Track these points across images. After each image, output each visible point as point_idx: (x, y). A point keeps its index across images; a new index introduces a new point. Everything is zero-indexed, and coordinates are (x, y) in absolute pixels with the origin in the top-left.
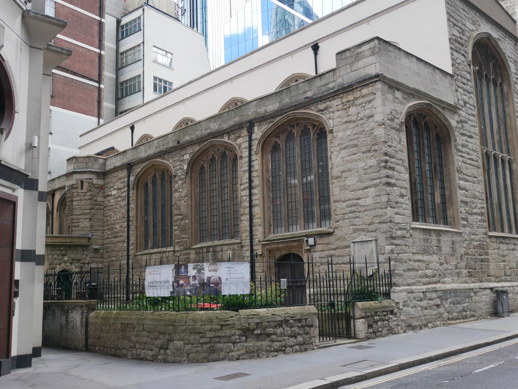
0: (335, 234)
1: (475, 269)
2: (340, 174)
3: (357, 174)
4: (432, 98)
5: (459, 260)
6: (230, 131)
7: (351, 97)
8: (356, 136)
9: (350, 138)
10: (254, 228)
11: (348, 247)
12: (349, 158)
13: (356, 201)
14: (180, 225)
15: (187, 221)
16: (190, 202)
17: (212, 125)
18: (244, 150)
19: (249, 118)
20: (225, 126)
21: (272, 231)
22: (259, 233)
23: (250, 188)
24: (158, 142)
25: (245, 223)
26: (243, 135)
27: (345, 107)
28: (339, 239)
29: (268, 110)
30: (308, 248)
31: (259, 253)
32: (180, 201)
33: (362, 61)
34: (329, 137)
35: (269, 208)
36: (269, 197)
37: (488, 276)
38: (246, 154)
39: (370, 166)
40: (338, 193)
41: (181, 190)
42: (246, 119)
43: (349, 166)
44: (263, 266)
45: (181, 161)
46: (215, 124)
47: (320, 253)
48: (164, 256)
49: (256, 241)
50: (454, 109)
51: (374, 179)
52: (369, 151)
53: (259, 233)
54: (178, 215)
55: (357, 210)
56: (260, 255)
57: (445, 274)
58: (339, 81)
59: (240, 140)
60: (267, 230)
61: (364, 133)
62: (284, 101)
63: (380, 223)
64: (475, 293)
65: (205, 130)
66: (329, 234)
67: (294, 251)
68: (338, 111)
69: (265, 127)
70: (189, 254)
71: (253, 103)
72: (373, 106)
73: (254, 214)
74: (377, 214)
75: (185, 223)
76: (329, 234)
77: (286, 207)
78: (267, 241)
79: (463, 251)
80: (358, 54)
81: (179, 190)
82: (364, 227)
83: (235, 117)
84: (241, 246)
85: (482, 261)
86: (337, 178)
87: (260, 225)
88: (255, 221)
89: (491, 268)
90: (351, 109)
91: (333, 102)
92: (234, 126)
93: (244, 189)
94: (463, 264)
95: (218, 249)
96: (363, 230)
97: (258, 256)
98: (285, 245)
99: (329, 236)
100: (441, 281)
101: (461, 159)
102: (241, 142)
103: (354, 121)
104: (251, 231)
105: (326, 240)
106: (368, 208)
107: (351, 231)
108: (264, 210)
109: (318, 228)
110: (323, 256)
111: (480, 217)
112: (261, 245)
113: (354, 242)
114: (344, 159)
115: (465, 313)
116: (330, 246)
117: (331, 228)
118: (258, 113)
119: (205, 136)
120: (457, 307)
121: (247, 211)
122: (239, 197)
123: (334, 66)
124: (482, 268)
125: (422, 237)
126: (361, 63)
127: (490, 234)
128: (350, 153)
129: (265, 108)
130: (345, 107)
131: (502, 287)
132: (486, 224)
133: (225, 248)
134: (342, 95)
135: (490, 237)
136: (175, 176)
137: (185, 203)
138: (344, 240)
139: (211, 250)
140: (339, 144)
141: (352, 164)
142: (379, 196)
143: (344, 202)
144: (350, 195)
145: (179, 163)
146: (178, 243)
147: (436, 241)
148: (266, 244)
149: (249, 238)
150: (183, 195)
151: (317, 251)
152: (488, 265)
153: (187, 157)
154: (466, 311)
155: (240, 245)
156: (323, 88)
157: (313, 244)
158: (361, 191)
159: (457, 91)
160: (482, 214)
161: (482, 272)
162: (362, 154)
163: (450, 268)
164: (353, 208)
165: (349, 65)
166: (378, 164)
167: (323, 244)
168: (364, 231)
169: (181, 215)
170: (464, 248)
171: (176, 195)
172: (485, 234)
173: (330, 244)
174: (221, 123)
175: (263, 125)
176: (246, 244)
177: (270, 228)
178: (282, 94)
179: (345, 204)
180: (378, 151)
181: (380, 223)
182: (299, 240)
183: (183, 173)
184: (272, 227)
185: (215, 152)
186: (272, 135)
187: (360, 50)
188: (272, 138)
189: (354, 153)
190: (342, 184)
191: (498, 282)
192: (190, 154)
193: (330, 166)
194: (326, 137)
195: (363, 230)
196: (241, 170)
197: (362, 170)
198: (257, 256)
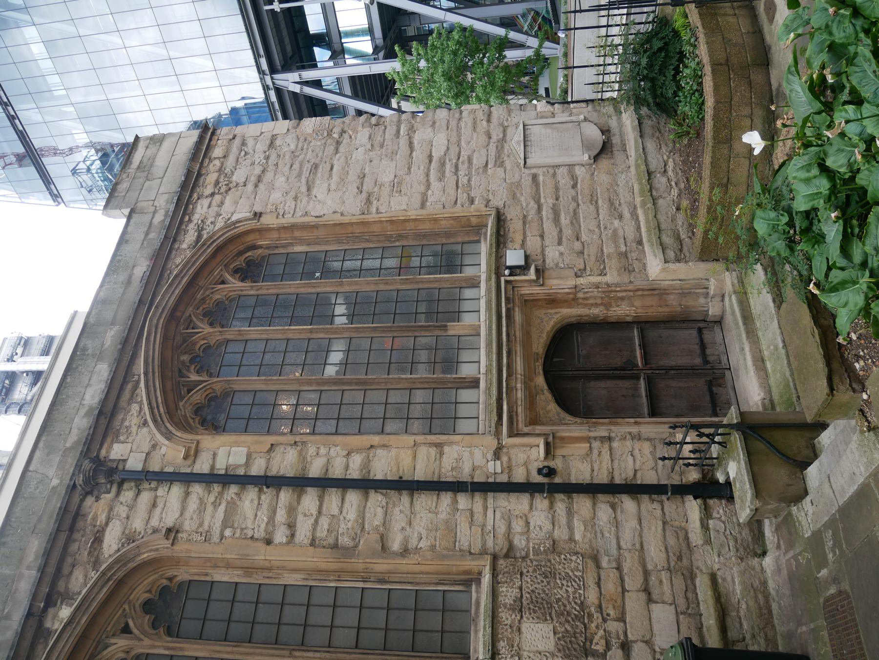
2: (364, 195)
3: (375, 162)
6: (53, 584)
8: (296, 166)
9: (295, 173)
10: (449, 476)
12: (335, 178)
13: (433, 164)
18: (154, 522)
22: (468, 453)
23: (300, 483)
25: (417, 524)
28: (514, 196)
39: (370, 138)
40: (405, 199)
43: (352, 177)
44: (588, 439)
47: (547, 242)
49: (493, 469)
51: (398, 131)
52: (338, 143)
53: (466, 455)
55: (454, 161)
61: (297, 154)
63: (489, 121)
66: (500, 219)
67: (539, 345)
74: (470, 124)
76: (500, 219)
80: (139, 167)
82: (492, 148)
84: (506, 556)
86: (369, 201)
96: (500, 149)
97: (552, 464)
98: (518, 348)
99: (504, 221)
102: (123, 522)
103: (263, 171)
106: (454, 139)
107: (500, 171)
110: (555, 233)
114: (333, 187)
116: (530, 218)
128: (327, 175)
129: (83, 411)
130: (223, 190)
138: (518, 185)
140: (296, 199)
141: (350, 172)
142: (434, 123)
143: (428, 186)
144: (418, 173)
155: (501, 562)
156: (152, 236)
158: (414, 154)
162: (338, 155)
164: (449, 167)
166: (371, 126)
168: (503, 147)
173: (525, 217)
175: (123, 420)
178: (85, 349)
179: (435, 185)
180: (346, 129)
181: (489, 121)
186: (172, 406)
188: (177, 407)
189: (329, 169)
190: (386, 190)
193: (338, 218)
195: (500, 149)
196: (216, 538)
197: (371, 153)
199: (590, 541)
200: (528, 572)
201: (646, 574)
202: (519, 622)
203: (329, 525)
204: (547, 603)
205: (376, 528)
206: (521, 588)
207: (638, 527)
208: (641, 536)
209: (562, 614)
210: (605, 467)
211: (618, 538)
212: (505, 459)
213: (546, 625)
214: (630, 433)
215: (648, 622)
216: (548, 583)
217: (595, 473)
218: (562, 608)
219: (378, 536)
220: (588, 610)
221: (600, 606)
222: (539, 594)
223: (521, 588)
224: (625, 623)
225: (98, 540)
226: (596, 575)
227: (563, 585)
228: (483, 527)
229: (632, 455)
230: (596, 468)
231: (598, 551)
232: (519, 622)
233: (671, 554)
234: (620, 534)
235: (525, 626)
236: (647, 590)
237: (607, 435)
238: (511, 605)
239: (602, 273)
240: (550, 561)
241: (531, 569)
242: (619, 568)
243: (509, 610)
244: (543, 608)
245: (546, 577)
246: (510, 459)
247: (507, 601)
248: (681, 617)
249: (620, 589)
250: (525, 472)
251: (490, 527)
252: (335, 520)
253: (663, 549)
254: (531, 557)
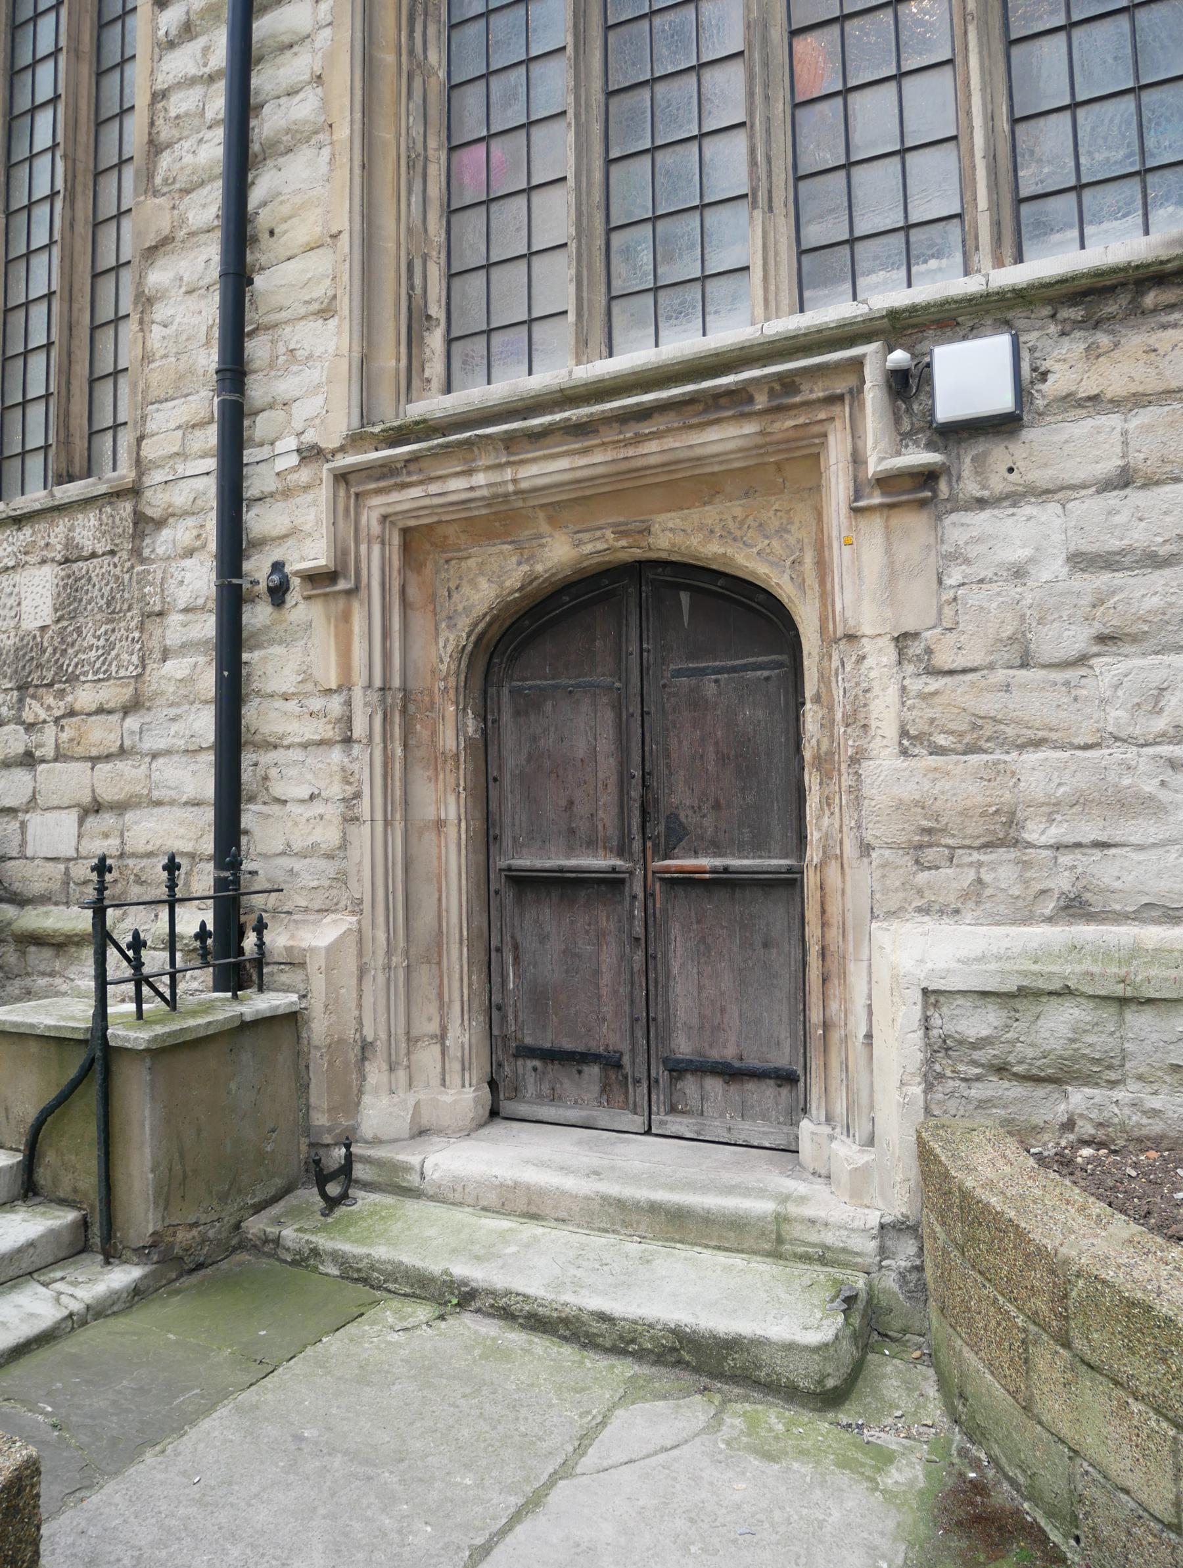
21: (435, 369)
30: (919, 457)
31: (313, 553)
35: (416, 163)
36: (416, 68)
44: (345, 686)
47: (1089, 507)
53: (315, 375)
56: (318, 579)
60: (389, 360)
67: (678, 534)
73: (263, 219)
77: (597, 129)
78: (398, 436)
84: (140, 519)
87: (326, 312)
88: (279, 282)
93: (188, 30)
98: (597, 459)
104: (234, 372)
108: (367, 167)
109: (999, 263)
112: (324, 493)
121: (207, 208)
122: (140, 98)
148: (385, 471)
149: (210, 437)
155: (126, 508)
176: (180, 497)
177: (413, 339)
182: (788, 384)
184: (435, 340)
198: (278, 594)
199: (162, 693)
200: (115, 566)
201: (120, 807)
202: (53, 560)
203: (187, 114)
204: (75, 610)
205: (183, 221)
206: (94, 555)
207: (184, 799)
208: (172, 803)
209: (63, 641)
210: (289, 729)
211: (168, 752)
212: (304, 476)
213: (50, 610)
214: (357, 795)
215: (56, 803)
216: (100, 608)
217: (279, 703)
218: (69, 640)
219: (166, 232)
220: (69, 689)
221: (72, 713)
222: (87, 592)
223: (94, 555)
224: (56, 760)
226: (111, 705)
227: (99, 638)
228: (182, 455)
229: (312, 797)
230: (292, 706)
231: (149, 709)
232: (53, 560)
233: (144, 862)
234: (175, 758)
236: (95, 807)
237: (355, 737)
238: (73, 538)
239: (910, 740)
240: (129, 609)
241: (118, 571)
242: (122, 752)
243: (67, 537)
244: (69, 603)
245: (109, 604)
246: (306, 488)
247: (78, 530)
248: (62, 867)
249: (94, 753)
250: (275, 533)
251: (181, 470)
252: (197, 121)
253: (150, 848)
254: (139, 568)
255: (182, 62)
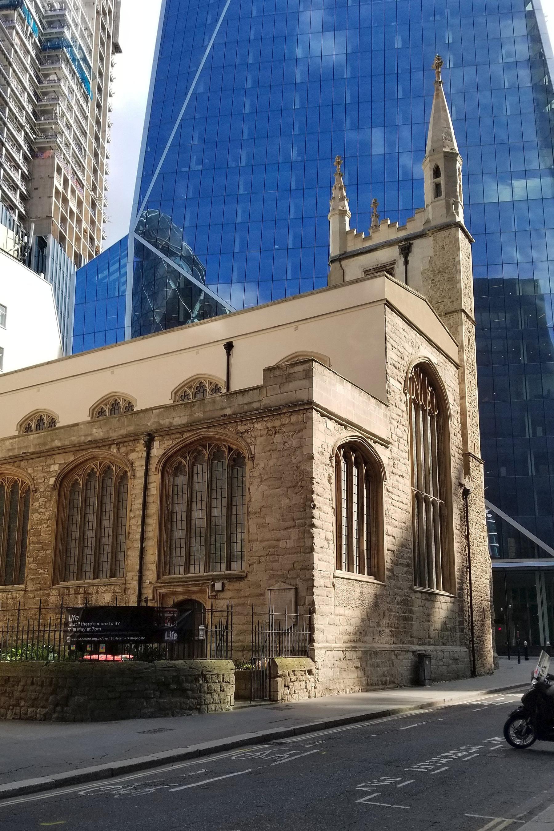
0: (249, 578)
1: (398, 628)
4: (365, 431)
5: (382, 616)
6: (121, 443)
7: (277, 423)
11: (263, 595)
14: (37, 557)
15: (48, 552)
16: (54, 527)
17: (95, 431)
19: (147, 430)
20: (114, 435)
21: (168, 571)
23: (144, 516)
24: (11, 444)
26: (138, 449)
27: (270, 432)
29: (175, 424)
32: (41, 524)
33: (294, 382)
34: (249, 465)
37: (411, 637)
38: (140, 473)
41: (43, 510)
42: (143, 429)
45: (47, 472)
46: (100, 430)
48: (10, 596)
50: (386, 444)
53: (152, 572)
54: (35, 543)
57: (366, 632)
58: (266, 401)
59: (132, 456)
62: (196, 416)
64: (396, 656)
65: (85, 436)
67: (194, 597)
68: (261, 436)
69: (168, 443)
70: (49, 594)
71: (154, 411)
72: (302, 437)
75: (46, 554)
78: (162, 583)
79: (386, 606)
80: (289, 374)
81: (39, 511)
83: (128, 426)
84: (125, 588)
85: (406, 619)
89: (414, 628)
90: (276, 436)
91: (256, 425)
92: (126, 436)
94: (385, 622)
95: (92, 590)
100: (362, 640)
101: (390, 501)
105: (236, 585)
111: (405, 569)
112: (152, 588)
113: (270, 590)
115: (385, 678)
117: (243, 572)
118: (160, 425)
119: (85, 444)
120: (377, 671)
121: (137, 545)
122: (127, 525)
123: (260, 382)
124: (405, 628)
125: (344, 587)
126: (292, 386)
127: (416, 588)
129: (171, 420)
130: (270, 432)
131: (425, 651)
132: (411, 577)
133: (101, 589)
134: (268, 418)
135: (416, 592)
136: (36, 491)
137: (48, 529)
139: (82, 591)
143: (261, 542)
145: (42, 475)
146: (33, 580)
147: (359, 594)
149: (137, 578)
150: (45, 517)
151: (224, 599)
152: (412, 625)
153: (55, 468)
154: (386, 676)
155: (123, 586)
156: (246, 407)
157: (220, 589)
159: (390, 423)
160: (408, 565)
161: (405, 631)
163: (371, 625)
165: (278, 385)
167: (231, 590)
169: (40, 543)
170: (387, 603)
171: (34, 517)
172: (411, 588)
174: (108, 431)
175: (166, 440)
176: (132, 586)
177: (165, 567)
179: (263, 544)
182: (203, 584)
183: (48, 489)
185: (96, 466)
187: (292, 371)
191: (421, 645)
192: (60, 464)
194: (244, 464)
225: (133, 451)
235: (110, 594)
255: (133, 522)
